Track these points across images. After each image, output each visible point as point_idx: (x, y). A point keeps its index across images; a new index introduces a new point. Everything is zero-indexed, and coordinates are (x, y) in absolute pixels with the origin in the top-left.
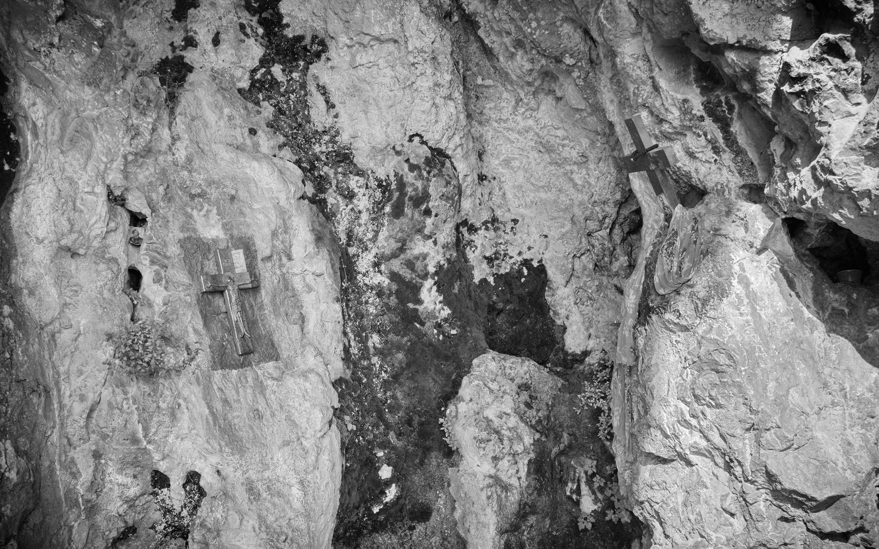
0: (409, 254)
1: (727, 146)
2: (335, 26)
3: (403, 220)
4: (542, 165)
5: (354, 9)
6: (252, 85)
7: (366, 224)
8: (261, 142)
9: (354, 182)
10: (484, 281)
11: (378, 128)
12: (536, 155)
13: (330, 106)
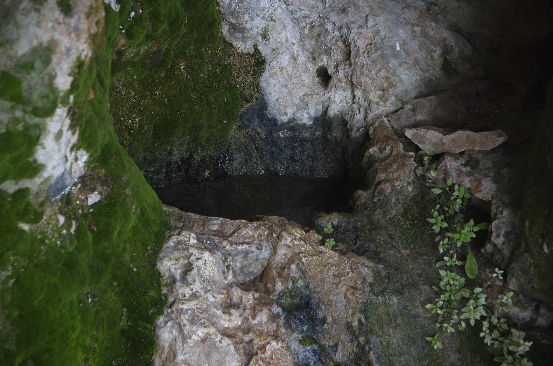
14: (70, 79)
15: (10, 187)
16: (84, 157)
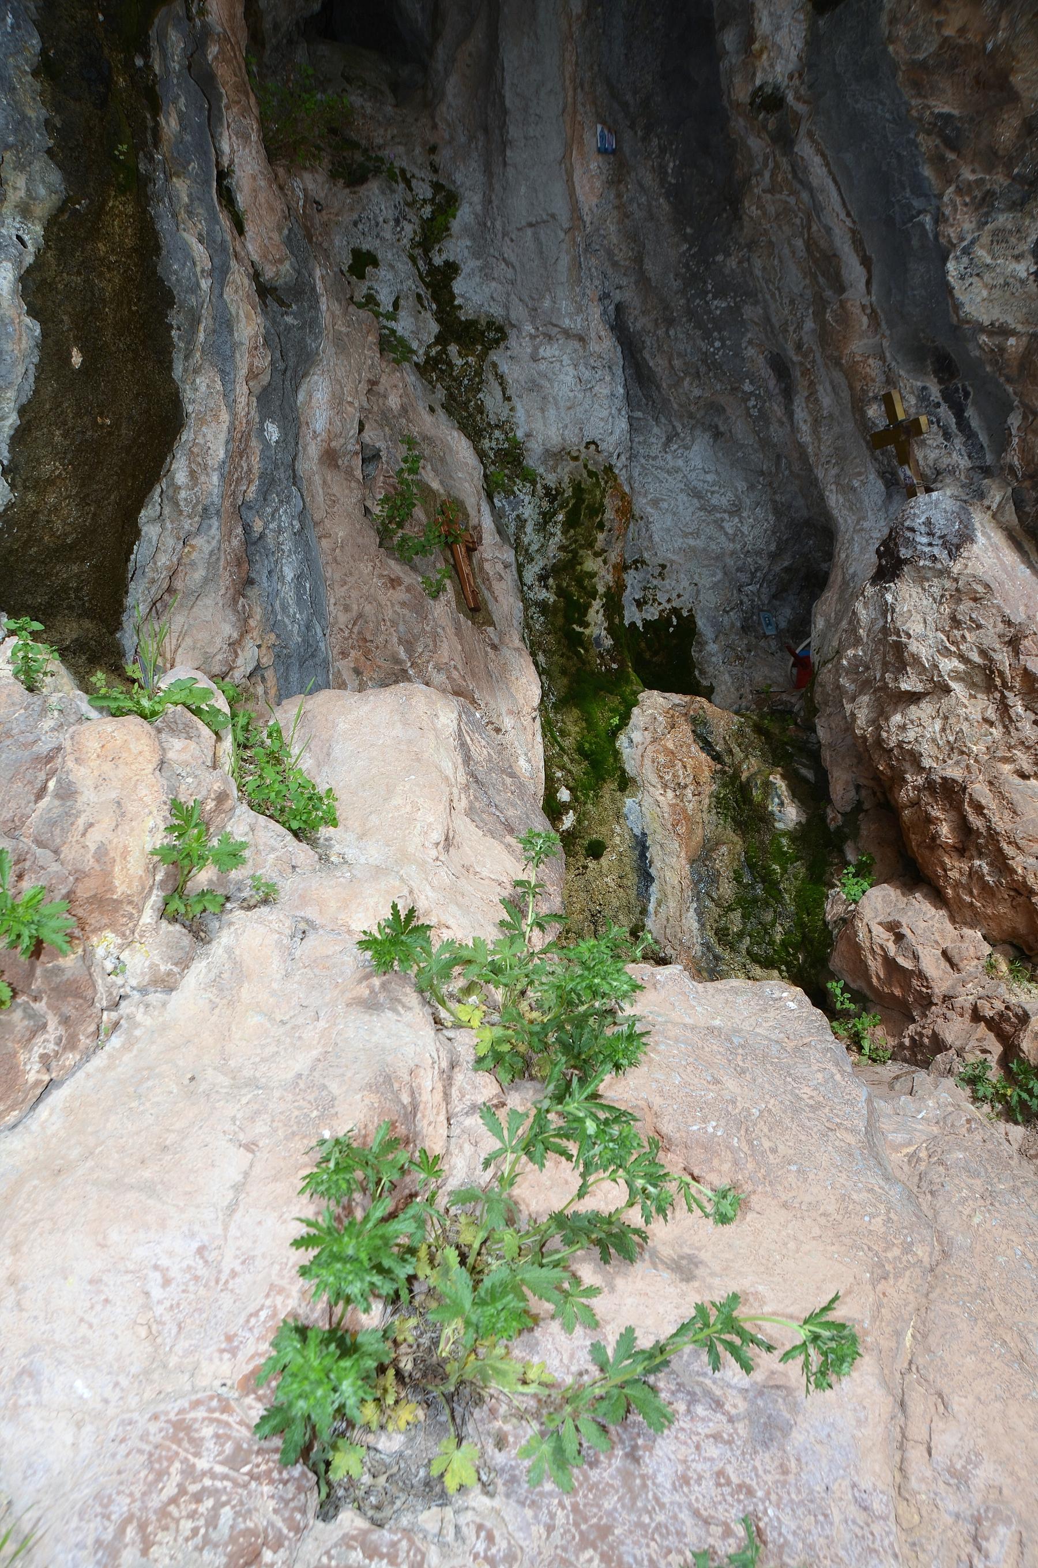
2: (518, 312)
4: (690, 510)
5: (544, 297)
6: (426, 362)
10: (633, 624)
11: (554, 429)
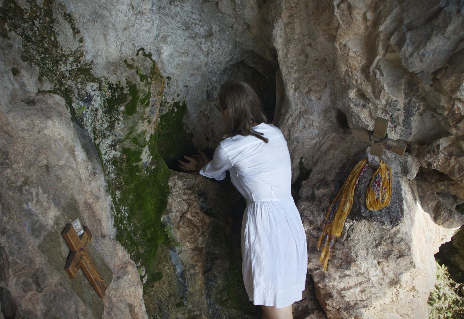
0: (134, 134)
1: (403, 124)
3: (135, 115)
4: (183, 39)
7: (101, 118)
8: (26, 82)
9: (90, 88)
11: (113, 46)
12: (181, 33)
13: (76, 31)
14: (149, 139)
15: (134, 164)
16: (151, 157)
